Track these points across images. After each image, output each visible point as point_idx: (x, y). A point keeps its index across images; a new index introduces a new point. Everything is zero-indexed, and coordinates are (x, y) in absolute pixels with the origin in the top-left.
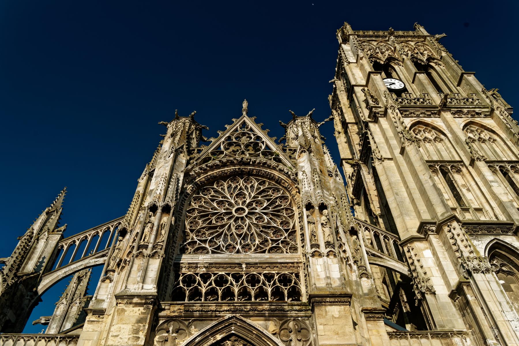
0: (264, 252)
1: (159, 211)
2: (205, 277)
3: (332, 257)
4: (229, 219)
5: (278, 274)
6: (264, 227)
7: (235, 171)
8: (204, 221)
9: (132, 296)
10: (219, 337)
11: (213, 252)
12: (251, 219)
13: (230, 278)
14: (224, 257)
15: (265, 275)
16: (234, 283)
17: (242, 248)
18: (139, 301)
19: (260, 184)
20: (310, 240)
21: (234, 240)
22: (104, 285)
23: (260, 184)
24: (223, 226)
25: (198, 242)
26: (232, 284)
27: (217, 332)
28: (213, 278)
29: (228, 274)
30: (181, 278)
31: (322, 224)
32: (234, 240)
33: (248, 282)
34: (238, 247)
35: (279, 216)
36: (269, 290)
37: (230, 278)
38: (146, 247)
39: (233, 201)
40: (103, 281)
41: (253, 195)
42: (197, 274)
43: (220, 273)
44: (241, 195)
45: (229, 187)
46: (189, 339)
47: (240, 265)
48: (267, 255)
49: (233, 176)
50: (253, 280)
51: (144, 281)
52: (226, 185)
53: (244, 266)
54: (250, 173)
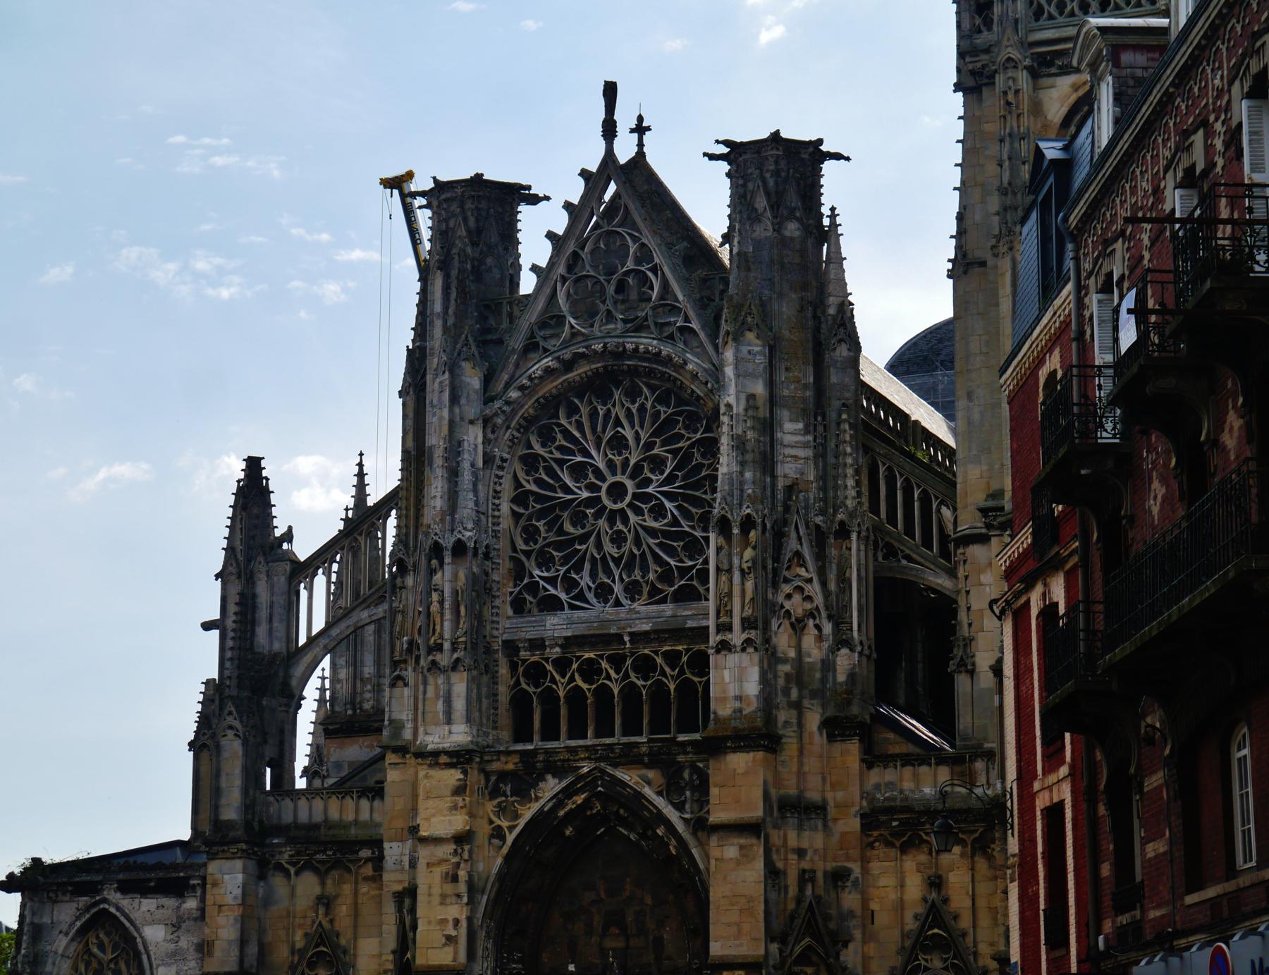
0: (663, 601)
1: (448, 559)
2: (562, 664)
3: (751, 650)
4: (597, 516)
5: (687, 650)
6: (666, 534)
7: (596, 373)
8: (549, 526)
9: (436, 754)
10: (580, 799)
11: (572, 607)
12: (638, 511)
13: (604, 664)
14: (595, 614)
15: (666, 655)
16: (612, 672)
17: (626, 590)
18: (448, 760)
19: (659, 400)
20: (718, 613)
21: (609, 573)
22: (397, 691)
23: (659, 400)
24: (583, 539)
25: (542, 582)
26: (608, 677)
27: (577, 792)
28: (575, 666)
29: (601, 656)
30: (521, 669)
31: (742, 571)
32: (609, 573)
33: (636, 669)
34: (618, 589)
35: (697, 502)
36: (672, 687)
37: (604, 664)
38: (439, 648)
39: (601, 465)
40: (393, 685)
41: (644, 437)
42: (547, 660)
43: (587, 655)
44: (619, 443)
45: (593, 414)
46: (535, 807)
47: (619, 638)
48: (668, 609)
49: (599, 386)
50: (645, 666)
51: (449, 721)
52: (585, 411)
53: (626, 639)
54: (634, 372)
